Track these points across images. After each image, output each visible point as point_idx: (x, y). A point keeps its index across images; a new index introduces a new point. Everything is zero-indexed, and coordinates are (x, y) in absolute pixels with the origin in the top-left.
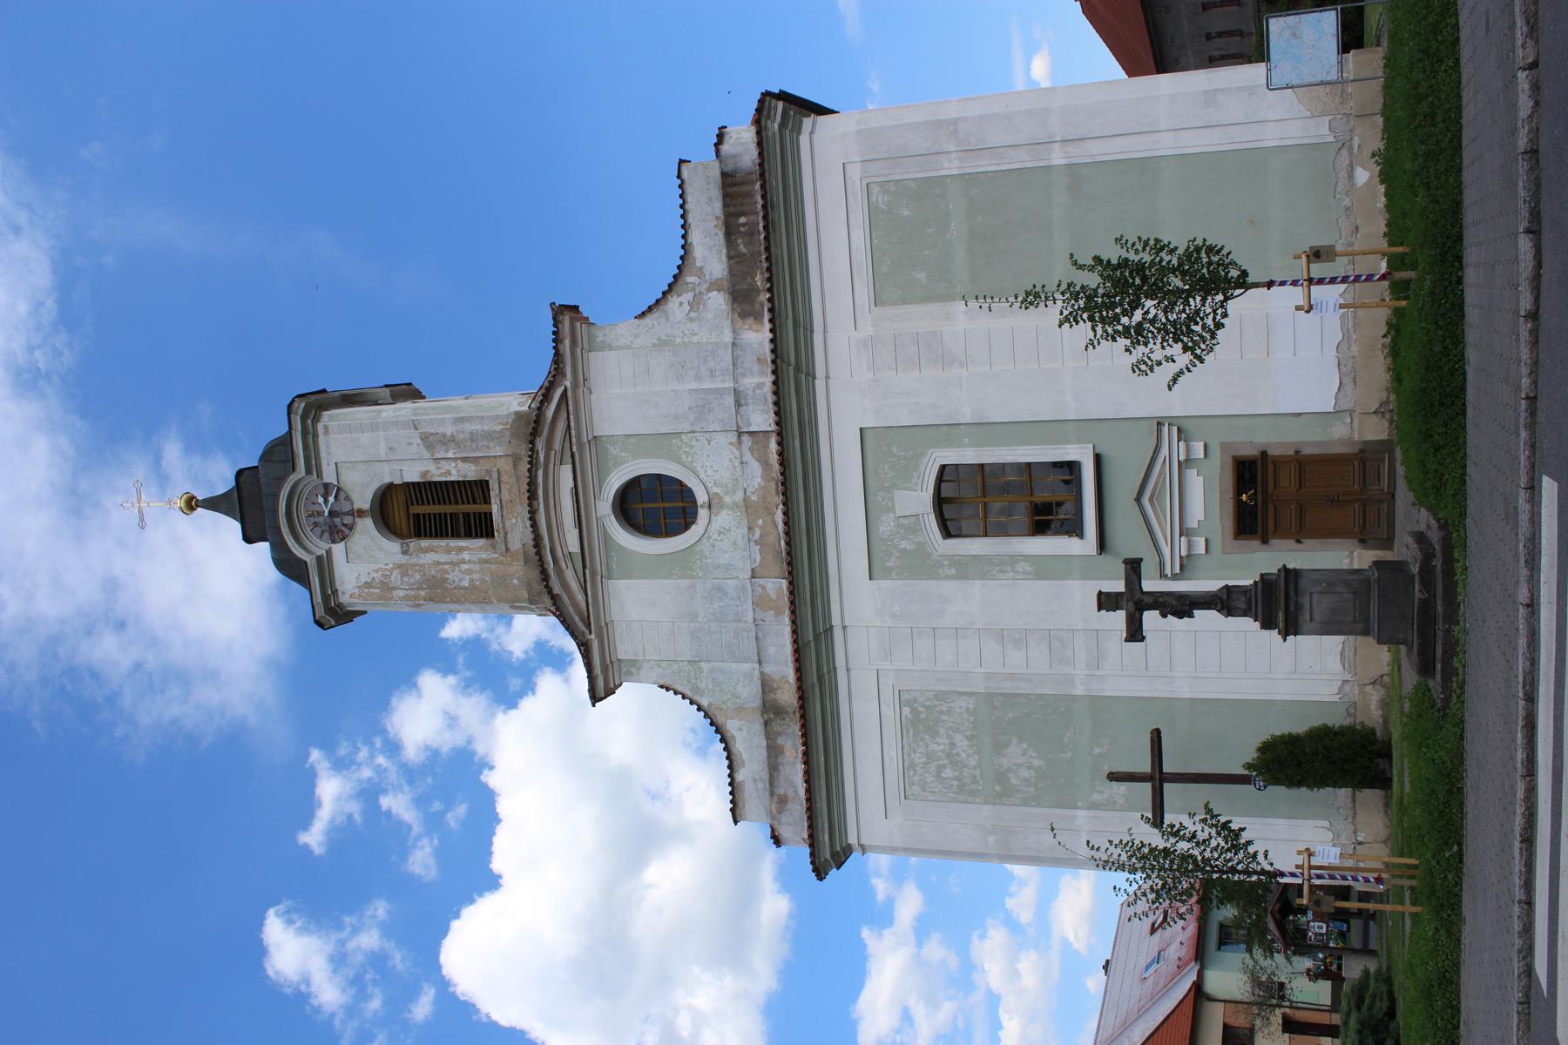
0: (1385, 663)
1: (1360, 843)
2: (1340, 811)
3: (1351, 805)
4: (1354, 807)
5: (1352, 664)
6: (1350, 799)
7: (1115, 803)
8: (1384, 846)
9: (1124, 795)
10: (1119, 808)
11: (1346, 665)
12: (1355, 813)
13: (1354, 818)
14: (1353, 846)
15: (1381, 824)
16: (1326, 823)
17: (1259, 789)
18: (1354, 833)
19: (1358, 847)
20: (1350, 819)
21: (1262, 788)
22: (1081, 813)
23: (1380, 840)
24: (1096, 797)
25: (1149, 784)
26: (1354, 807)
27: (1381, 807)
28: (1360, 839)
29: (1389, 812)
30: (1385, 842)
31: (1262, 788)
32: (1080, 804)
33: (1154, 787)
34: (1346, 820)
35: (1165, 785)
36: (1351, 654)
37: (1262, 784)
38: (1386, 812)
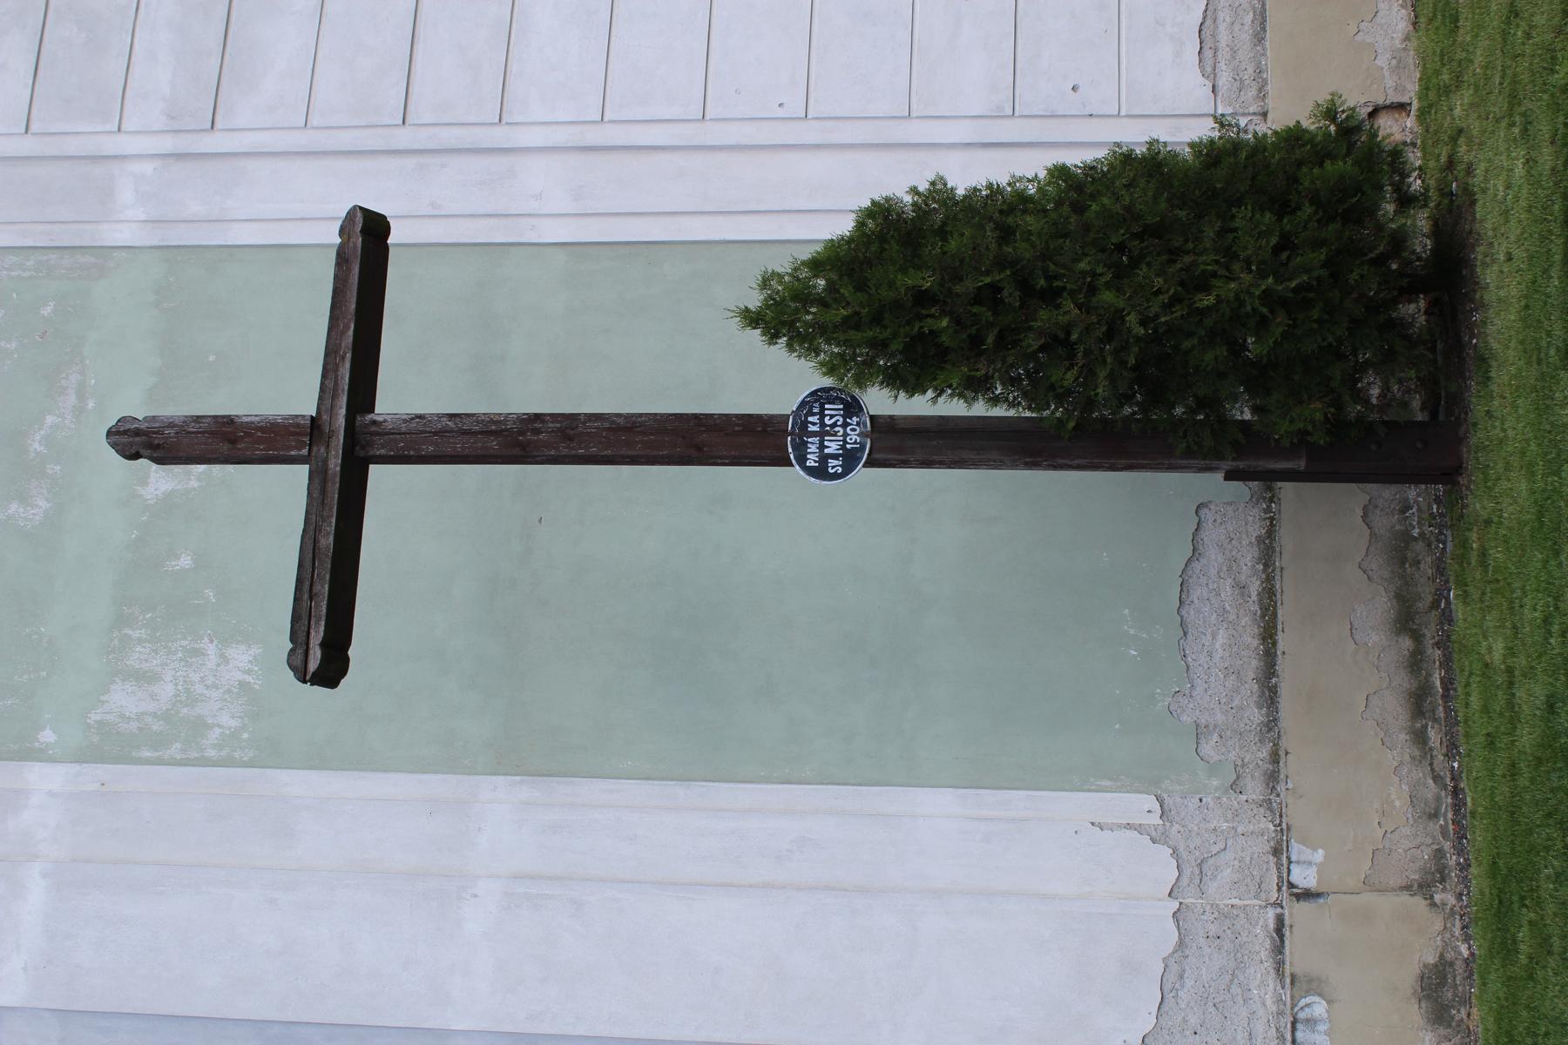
0: (1382, 61)
1: (1307, 895)
2: (1208, 748)
3: (1256, 716)
4: (1271, 723)
5: (1248, 75)
6: (1252, 687)
7: (200, 726)
8: (1419, 903)
9: (243, 685)
10: (212, 753)
11: (1224, 79)
12: (1275, 758)
13: (1272, 778)
14: (1271, 914)
15: (1398, 796)
16: (1142, 807)
17: (820, 472)
18: (1276, 852)
19: (1298, 913)
20: (1254, 788)
21: (835, 466)
22: (45, 779)
23: (1396, 881)
24: (124, 701)
25: (299, 475)
26: (1271, 723)
27: (1394, 708)
28: (1304, 877)
29: (1434, 736)
30: (1424, 887)
31: (835, 466)
32: (47, 736)
33: (318, 479)
34: (1236, 787)
35: (378, 475)
36: (1245, 36)
37: (832, 447)
38: (1420, 738)
